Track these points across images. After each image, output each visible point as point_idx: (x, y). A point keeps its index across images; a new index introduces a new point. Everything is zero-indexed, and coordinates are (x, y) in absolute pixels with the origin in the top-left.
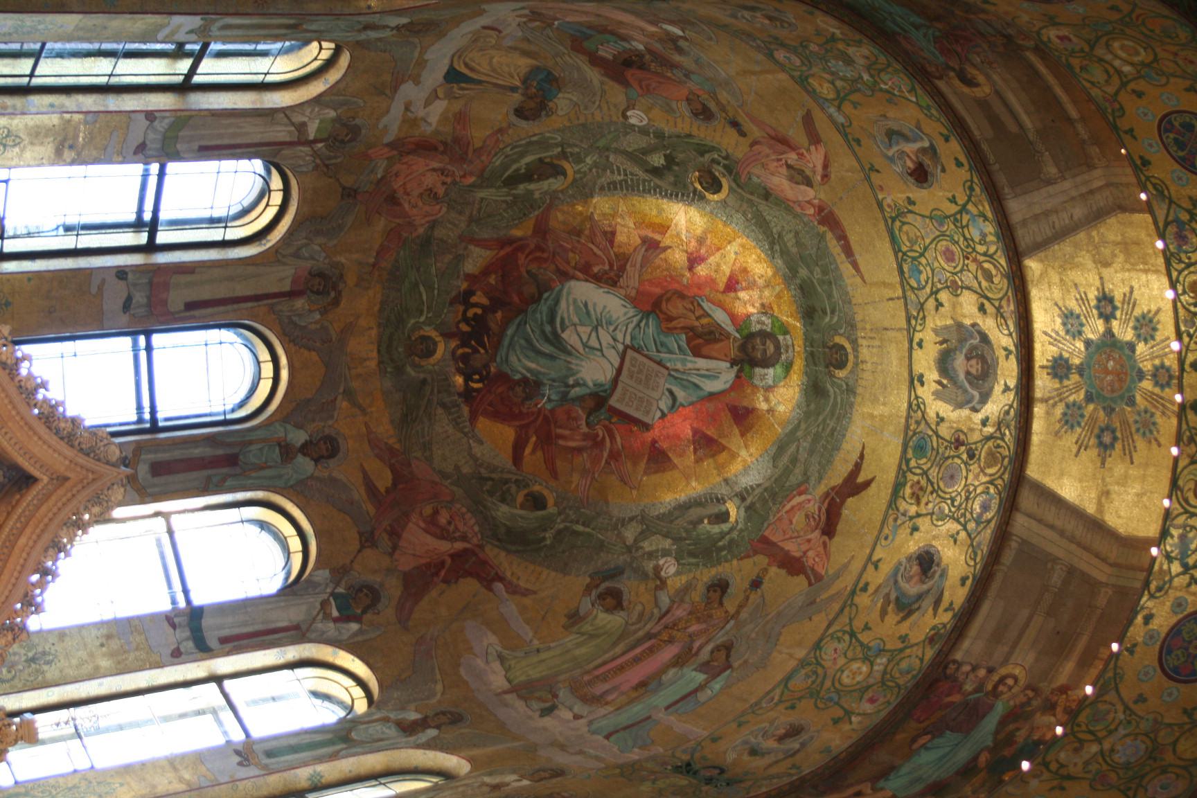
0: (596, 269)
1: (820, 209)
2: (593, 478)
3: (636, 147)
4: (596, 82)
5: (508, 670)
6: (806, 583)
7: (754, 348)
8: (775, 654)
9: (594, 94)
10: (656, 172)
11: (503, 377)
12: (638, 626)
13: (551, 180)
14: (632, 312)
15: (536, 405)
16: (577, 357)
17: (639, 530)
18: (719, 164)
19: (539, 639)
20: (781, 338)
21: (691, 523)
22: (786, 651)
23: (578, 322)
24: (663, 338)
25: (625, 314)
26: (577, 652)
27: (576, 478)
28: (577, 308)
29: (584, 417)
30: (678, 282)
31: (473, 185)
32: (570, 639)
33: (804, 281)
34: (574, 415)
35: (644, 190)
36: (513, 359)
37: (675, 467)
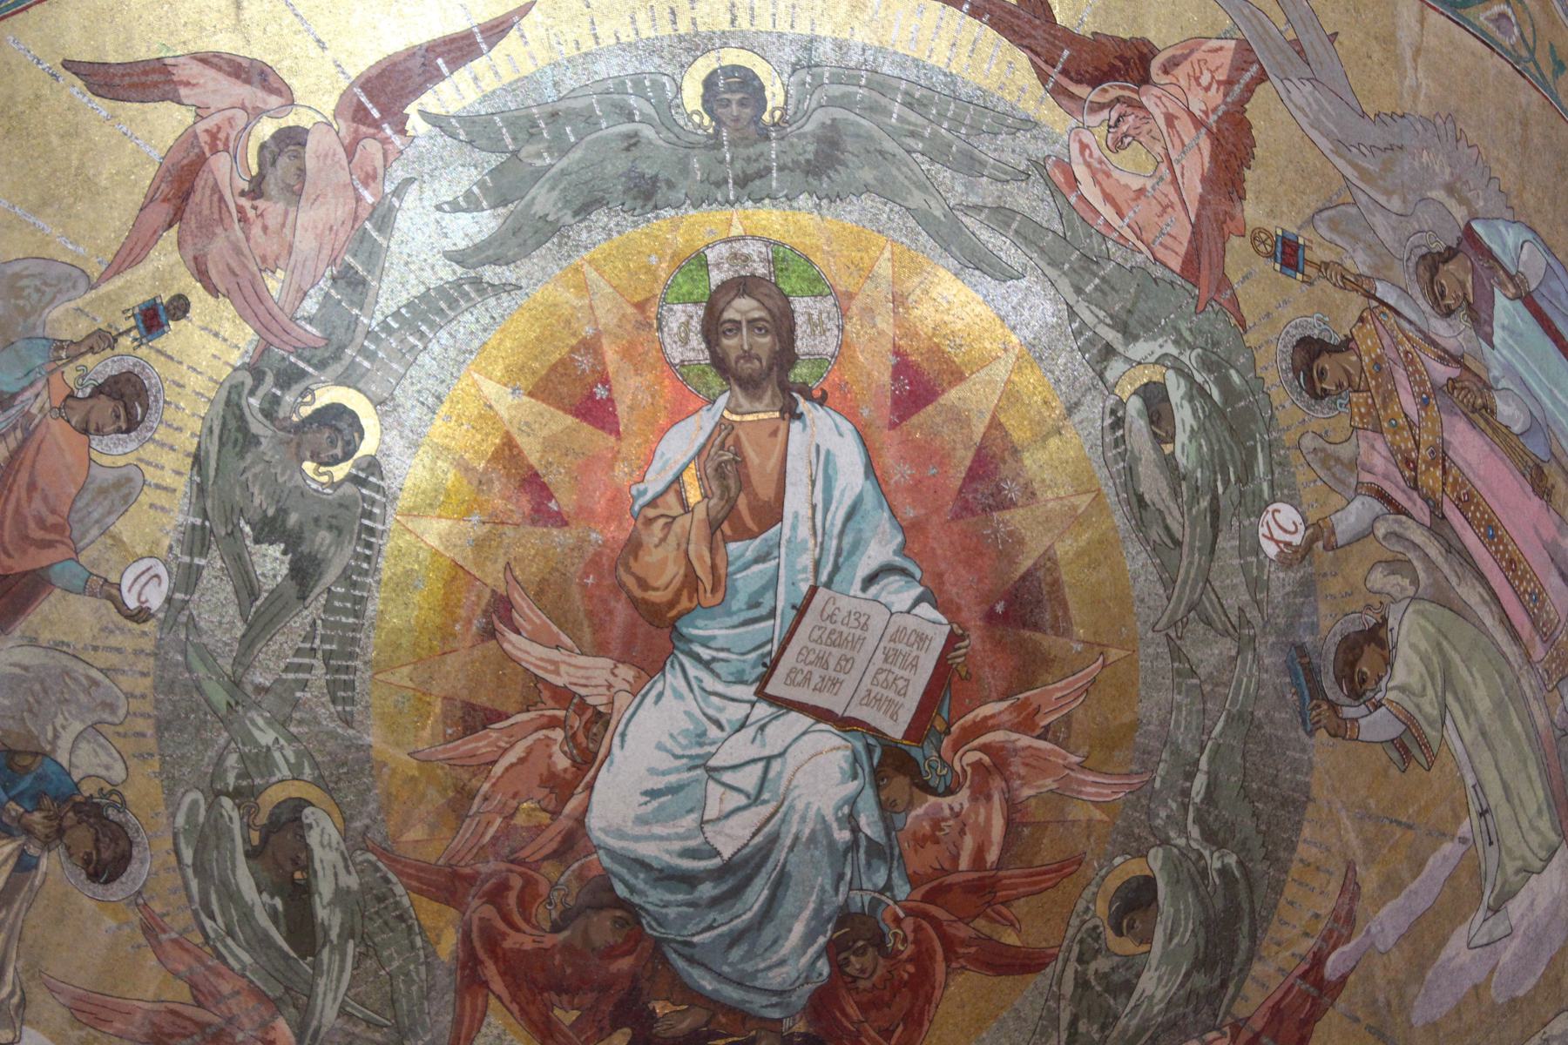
0: (562, 762)
1: (359, 115)
2: (1081, 766)
3: (232, 610)
4: (27, 656)
5: (1527, 872)
6: (1261, 91)
7: (747, 356)
8: (1422, 109)
9: (66, 672)
10: (304, 572)
11: (822, 1002)
12: (1418, 564)
13: (313, 838)
14: (673, 678)
15: (898, 921)
16: (783, 821)
17: (1201, 628)
18: (276, 401)
19: (1458, 820)
20: (716, 277)
21: (1176, 493)
22: (1410, 72)
23: (695, 816)
24: (739, 602)
25: (678, 696)
26: (1484, 704)
27: (1077, 812)
28: (658, 817)
29: (932, 799)
30: (599, 554)
31: (300, 1030)
32: (1457, 738)
33: (567, 203)
34: (927, 827)
35: (356, 615)
36: (776, 978)
37: (1049, 558)
